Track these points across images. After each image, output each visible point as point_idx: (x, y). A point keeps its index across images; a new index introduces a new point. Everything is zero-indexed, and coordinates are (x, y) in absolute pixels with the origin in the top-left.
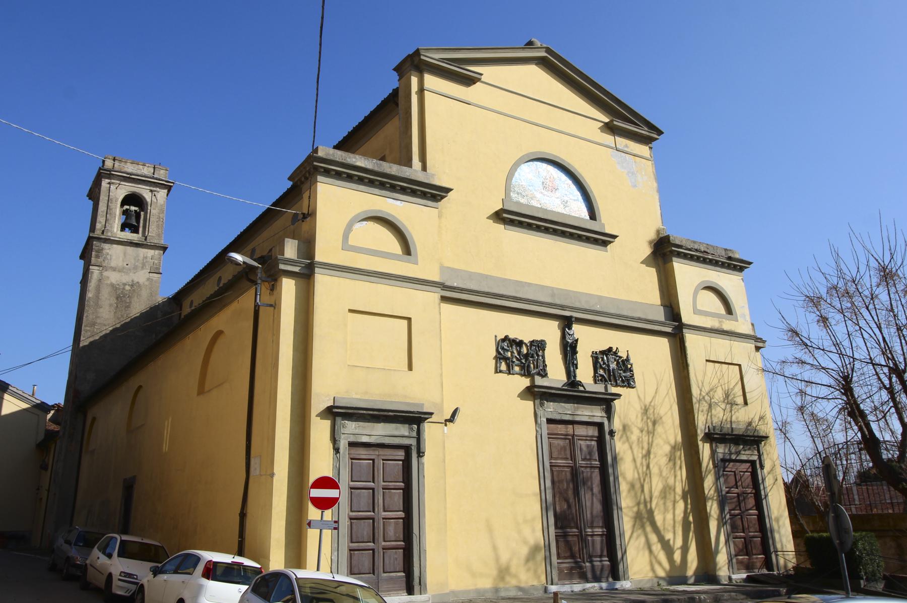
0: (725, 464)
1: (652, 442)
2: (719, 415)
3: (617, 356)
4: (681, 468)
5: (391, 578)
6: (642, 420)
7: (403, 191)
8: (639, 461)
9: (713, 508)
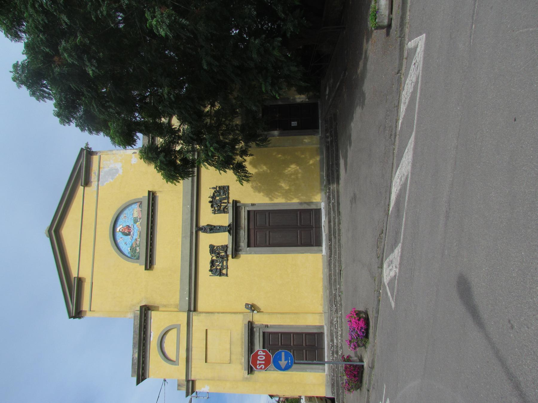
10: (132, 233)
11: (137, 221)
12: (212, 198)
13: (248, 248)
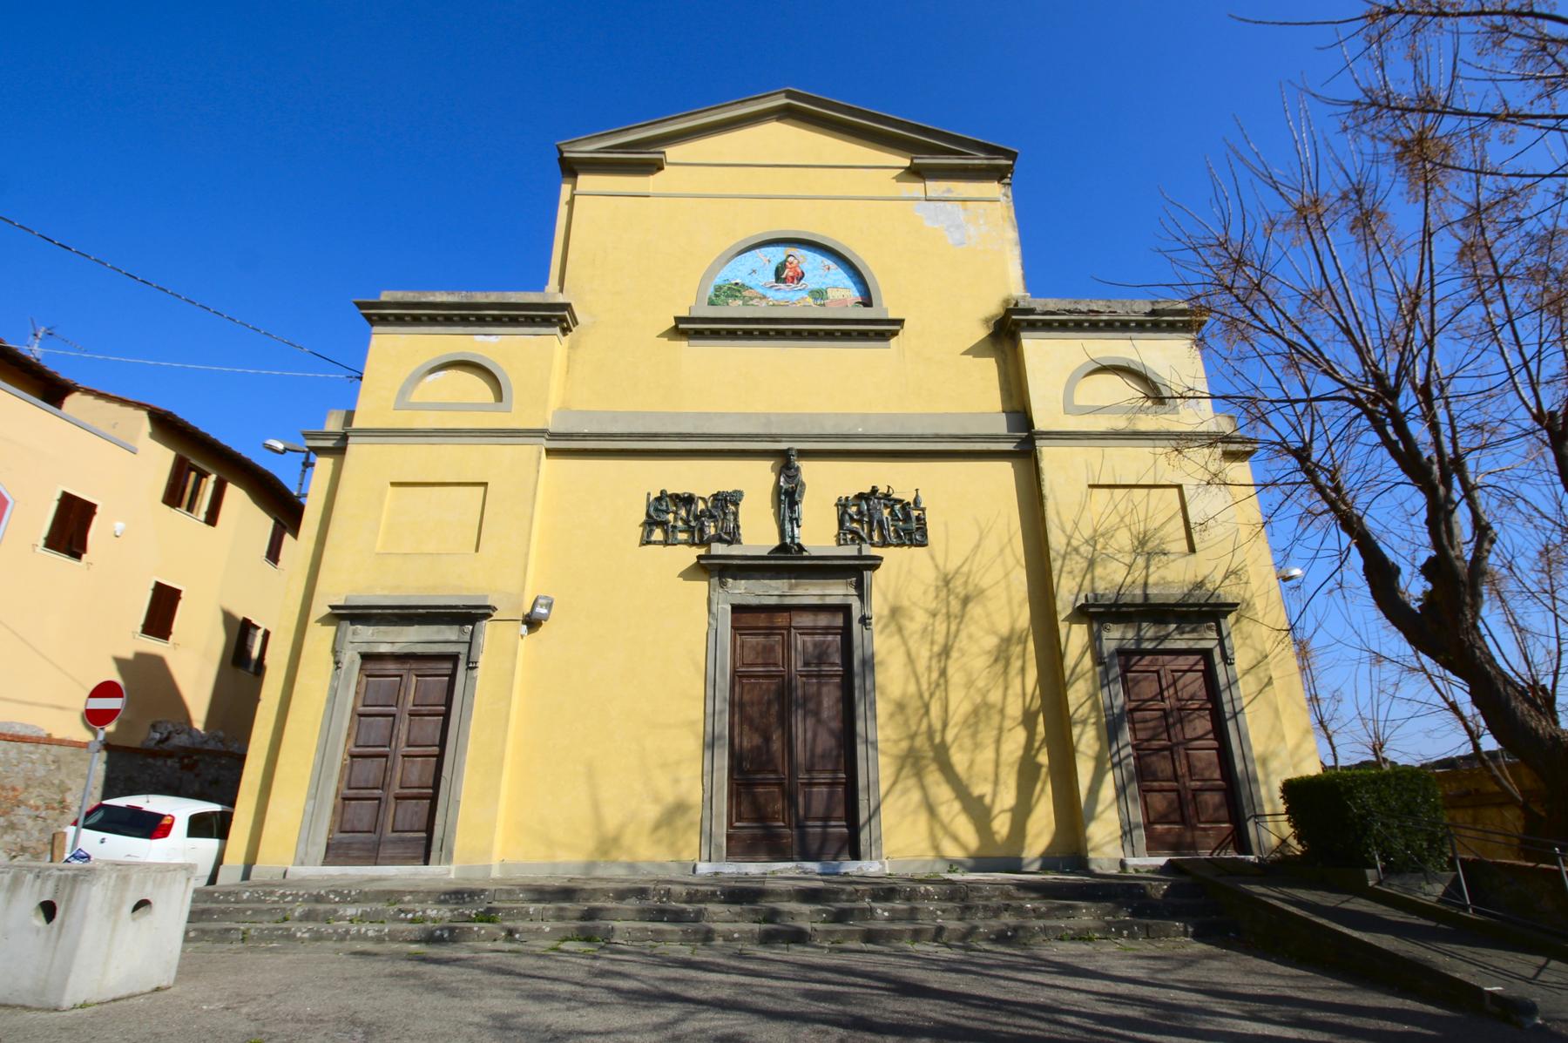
0: (1128, 660)
1: (958, 631)
2: (1113, 577)
3: (889, 500)
4: (1023, 670)
5: (403, 840)
6: (937, 597)
7: (498, 321)
8: (922, 665)
9: (1087, 741)
10: (782, 286)
11: (815, 299)
12: (887, 496)
13: (729, 608)
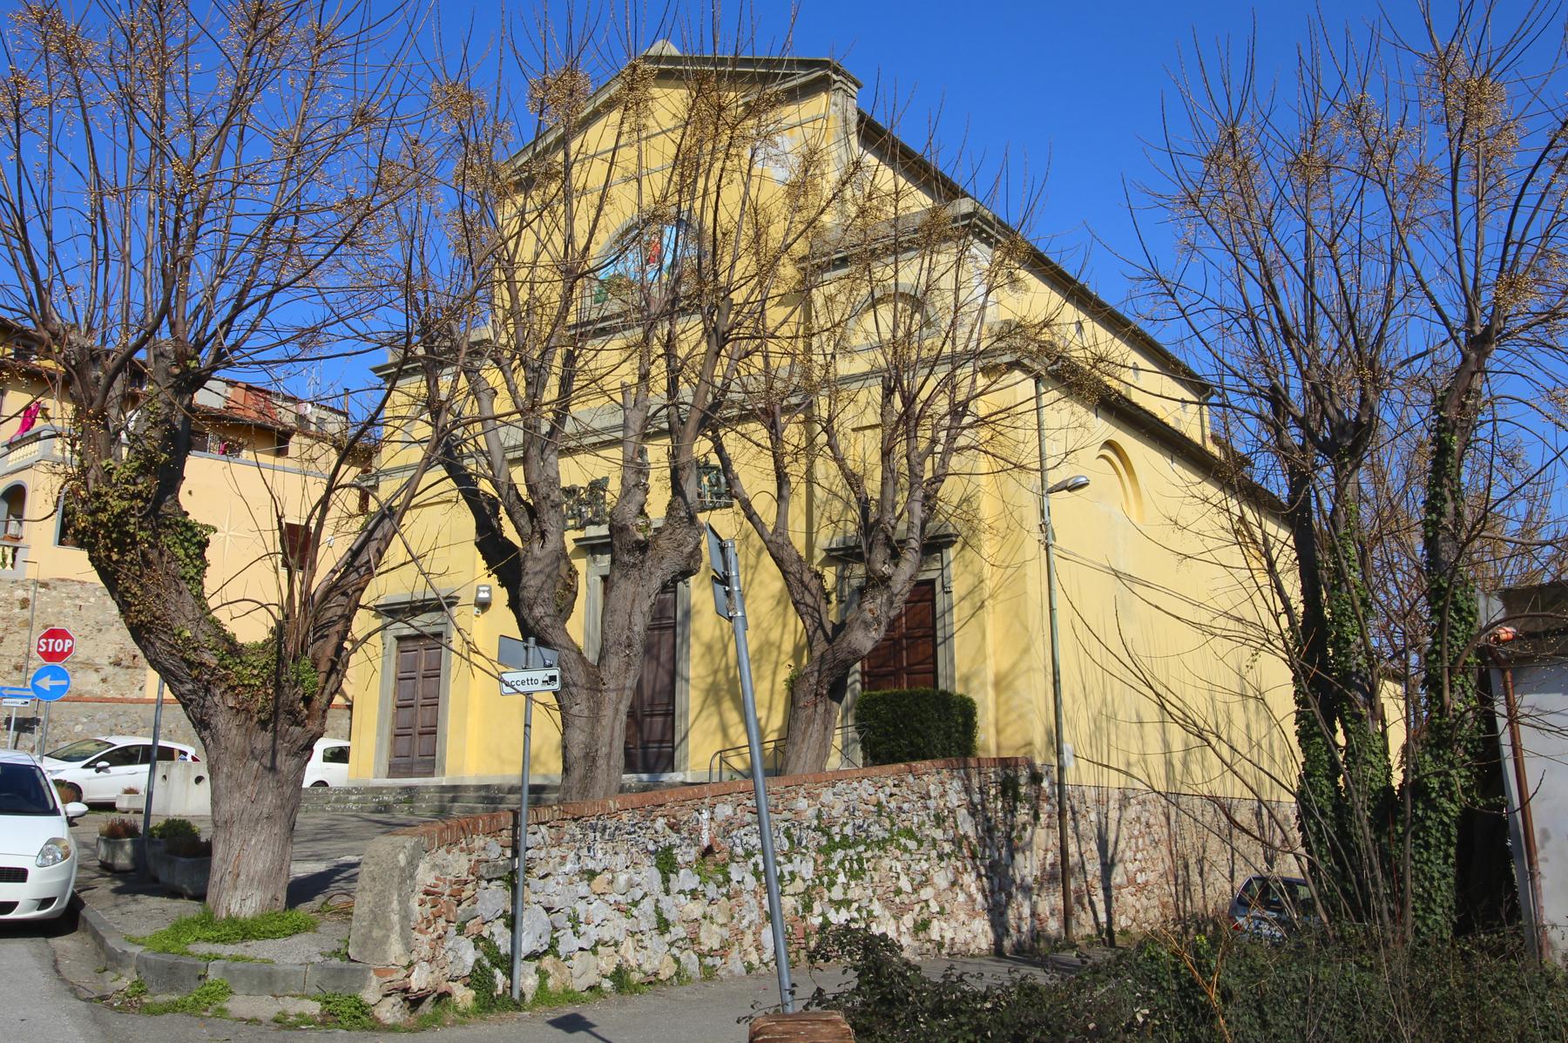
1: (752, 580)
5: (424, 762)
13: (599, 579)
